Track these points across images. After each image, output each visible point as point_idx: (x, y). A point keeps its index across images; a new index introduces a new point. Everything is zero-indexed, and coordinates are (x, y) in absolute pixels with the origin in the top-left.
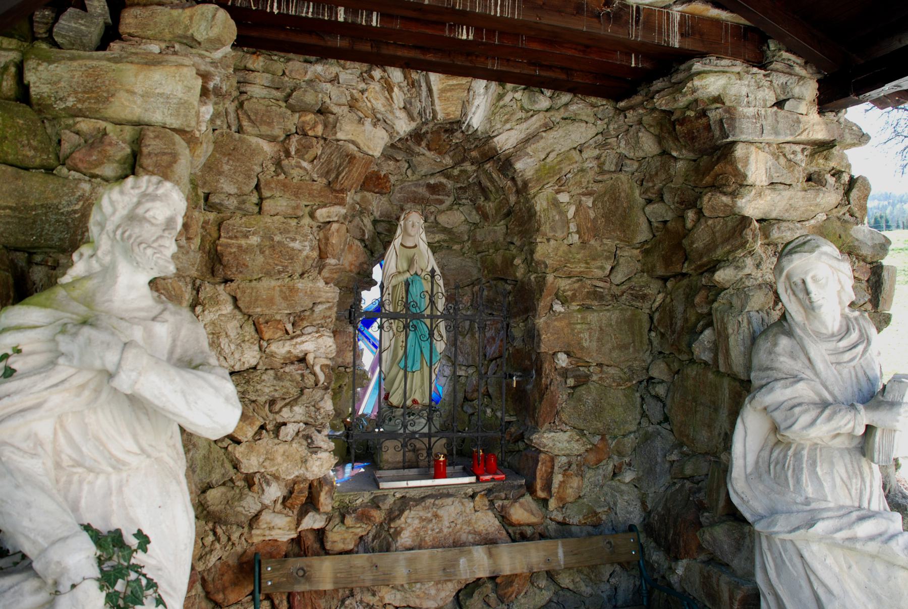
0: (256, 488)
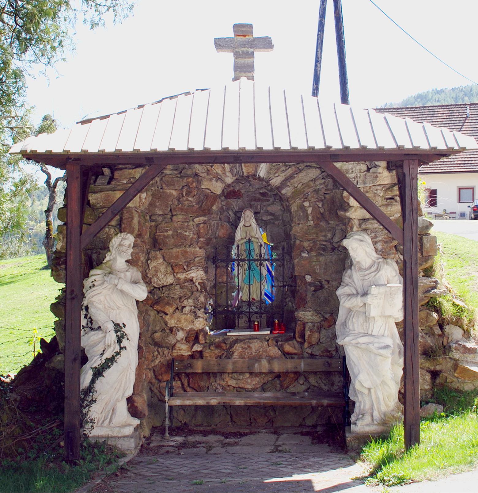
0: (173, 332)
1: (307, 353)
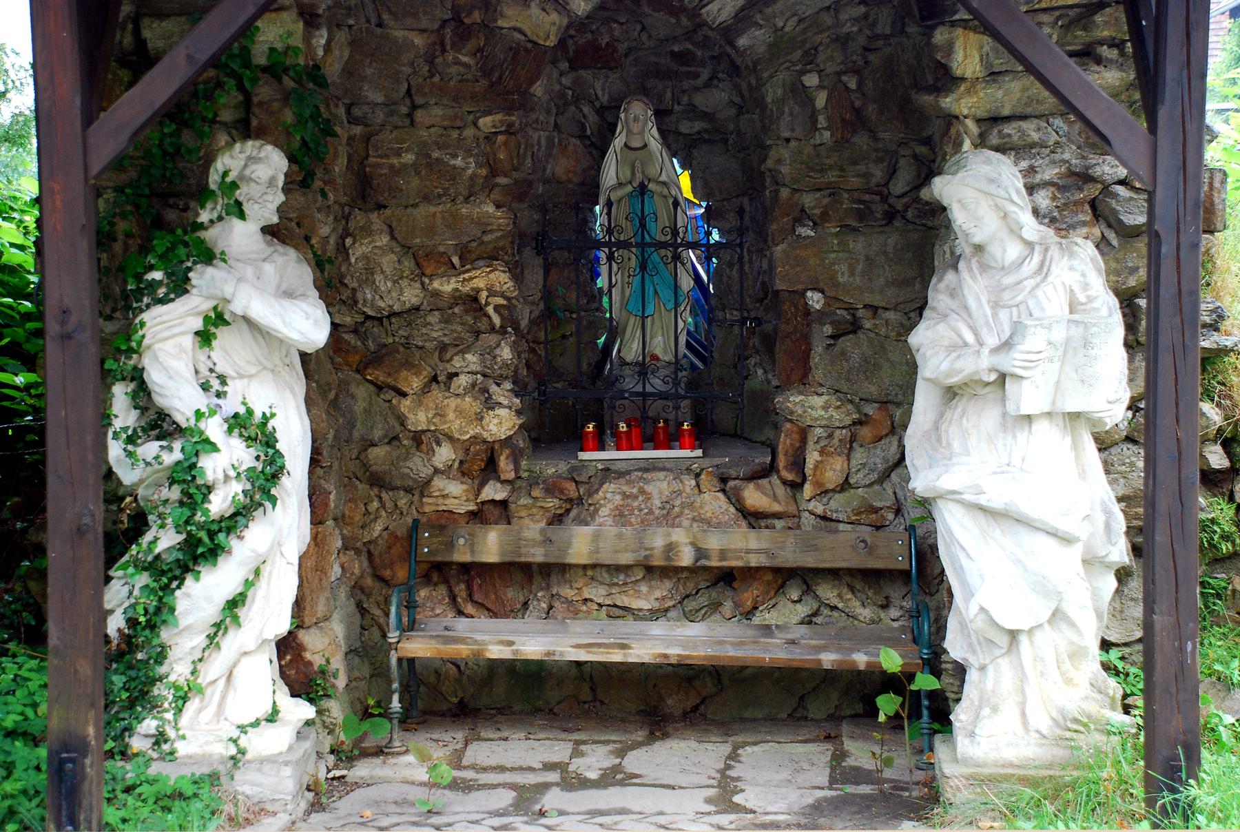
0: (424, 447)
1: (812, 513)
